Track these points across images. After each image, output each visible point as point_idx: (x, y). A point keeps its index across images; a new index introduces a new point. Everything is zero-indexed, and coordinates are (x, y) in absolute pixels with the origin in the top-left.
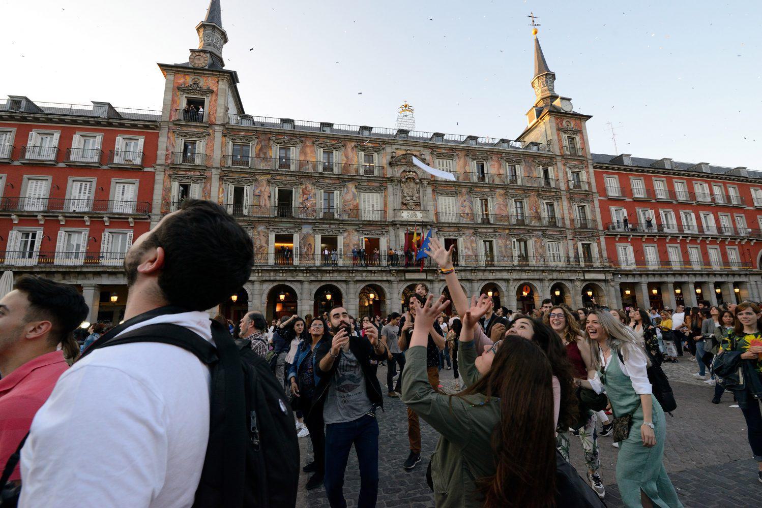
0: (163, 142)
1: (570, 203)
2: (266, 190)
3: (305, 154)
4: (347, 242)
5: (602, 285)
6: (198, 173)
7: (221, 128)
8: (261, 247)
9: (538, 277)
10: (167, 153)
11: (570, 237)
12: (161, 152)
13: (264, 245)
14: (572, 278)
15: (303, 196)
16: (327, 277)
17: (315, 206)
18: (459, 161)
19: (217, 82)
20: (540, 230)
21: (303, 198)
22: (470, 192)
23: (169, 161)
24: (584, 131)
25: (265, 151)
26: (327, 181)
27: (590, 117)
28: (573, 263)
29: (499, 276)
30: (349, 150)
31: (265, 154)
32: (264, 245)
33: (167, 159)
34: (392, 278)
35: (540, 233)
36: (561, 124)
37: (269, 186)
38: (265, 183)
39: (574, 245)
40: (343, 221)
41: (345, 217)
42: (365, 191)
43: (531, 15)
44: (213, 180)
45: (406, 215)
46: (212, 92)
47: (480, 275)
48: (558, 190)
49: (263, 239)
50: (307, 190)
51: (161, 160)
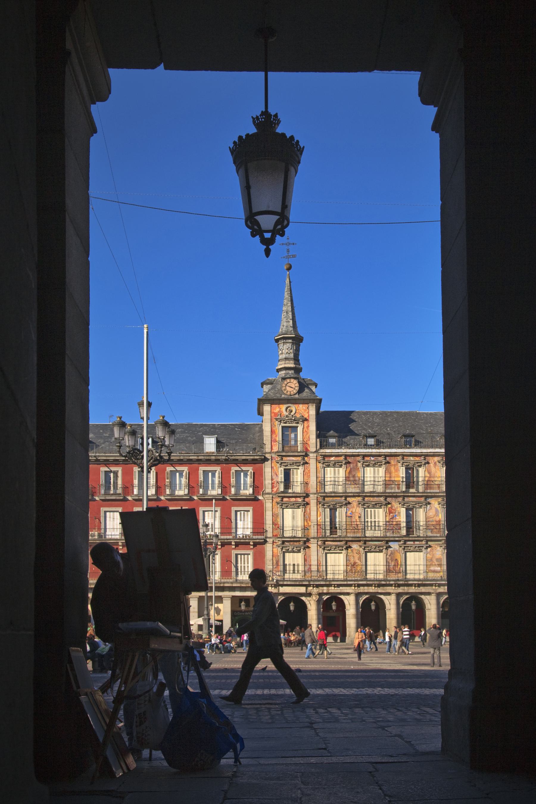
2: (357, 511)
7: (315, 455)
8: (355, 563)
12: (268, 482)
13: (357, 561)
16: (412, 590)
19: (308, 408)
23: (275, 489)
26: (411, 499)
30: (432, 465)
31: (354, 476)
38: (355, 504)
40: (427, 537)
44: (311, 505)
50: (393, 508)
51: (268, 490)
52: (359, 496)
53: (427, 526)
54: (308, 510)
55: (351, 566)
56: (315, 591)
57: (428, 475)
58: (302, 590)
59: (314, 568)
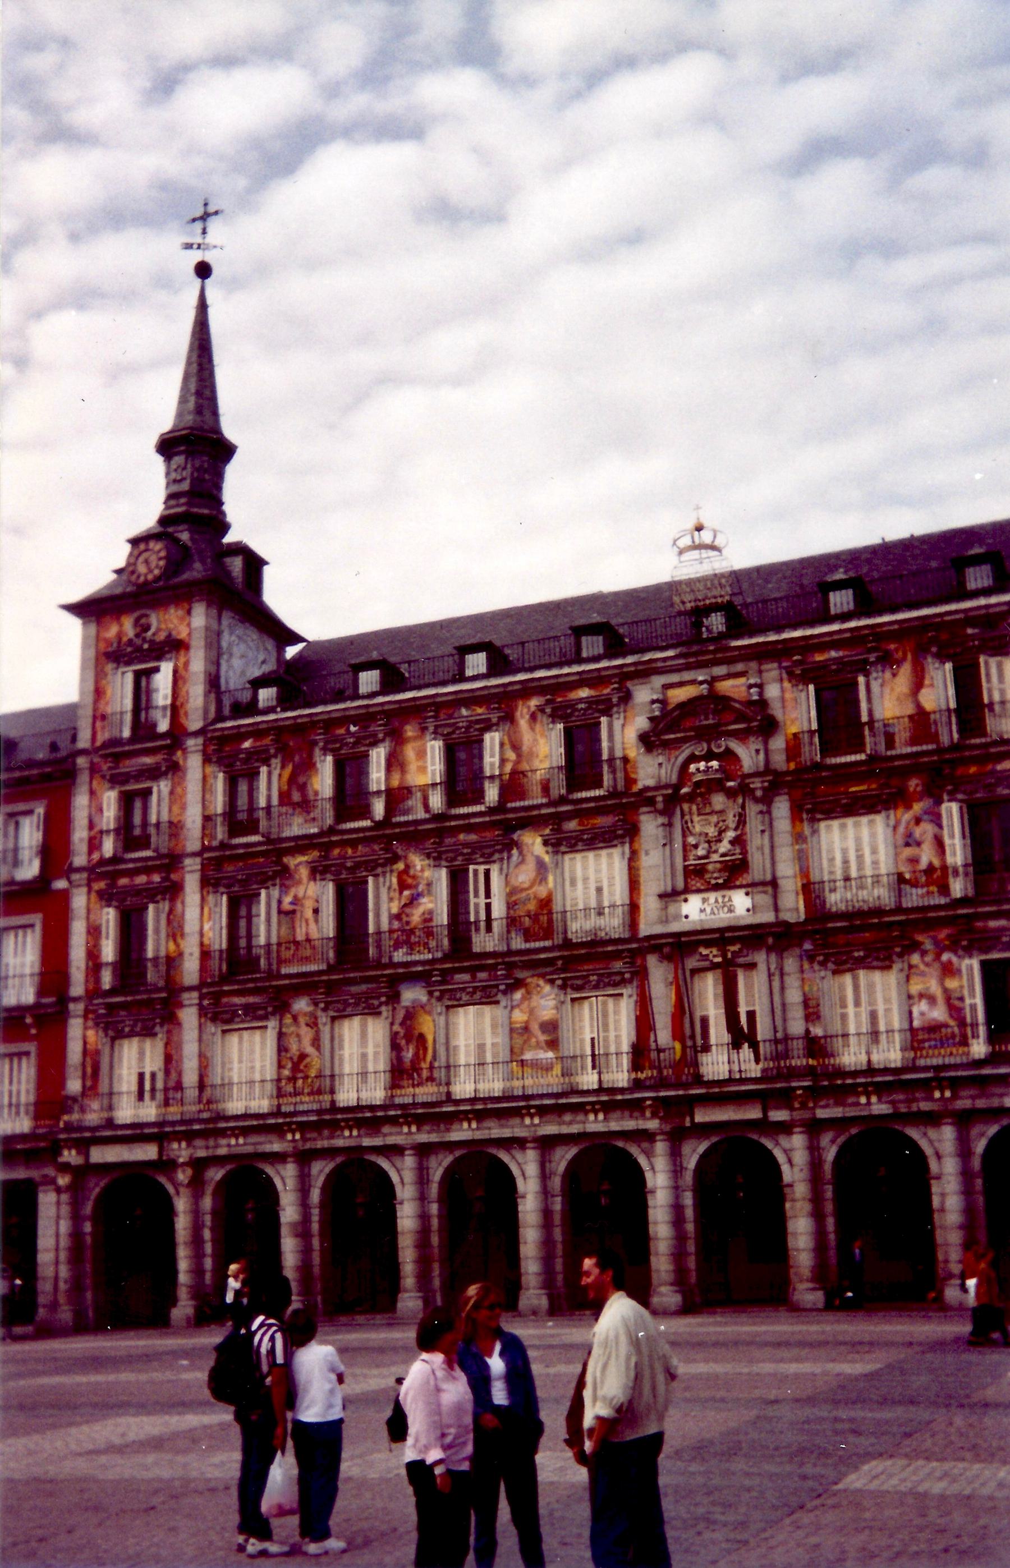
3: (403, 767)
4: (519, 1016)
6: (156, 878)
8: (303, 1056)
10: (93, 833)
12: (80, 835)
13: (310, 1050)
15: (401, 893)
17: (431, 920)
18: (894, 675)
21: (400, 900)
23: (96, 856)
25: (301, 780)
26: (462, 837)
30: (523, 723)
31: (303, 788)
32: (310, 1050)
34: (653, 1125)
37: (315, 880)
38: (304, 872)
40: (510, 953)
41: (518, 943)
42: (573, 849)
45: (696, 911)
46: (175, 646)
49: (307, 1034)
50: (412, 872)
51: (80, 859)
52: (312, 847)
53: (512, 922)
54: (179, 905)
55: (293, 1067)
56: (181, 1151)
57: (511, 755)
58: (148, 1152)
59: (190, 1078)
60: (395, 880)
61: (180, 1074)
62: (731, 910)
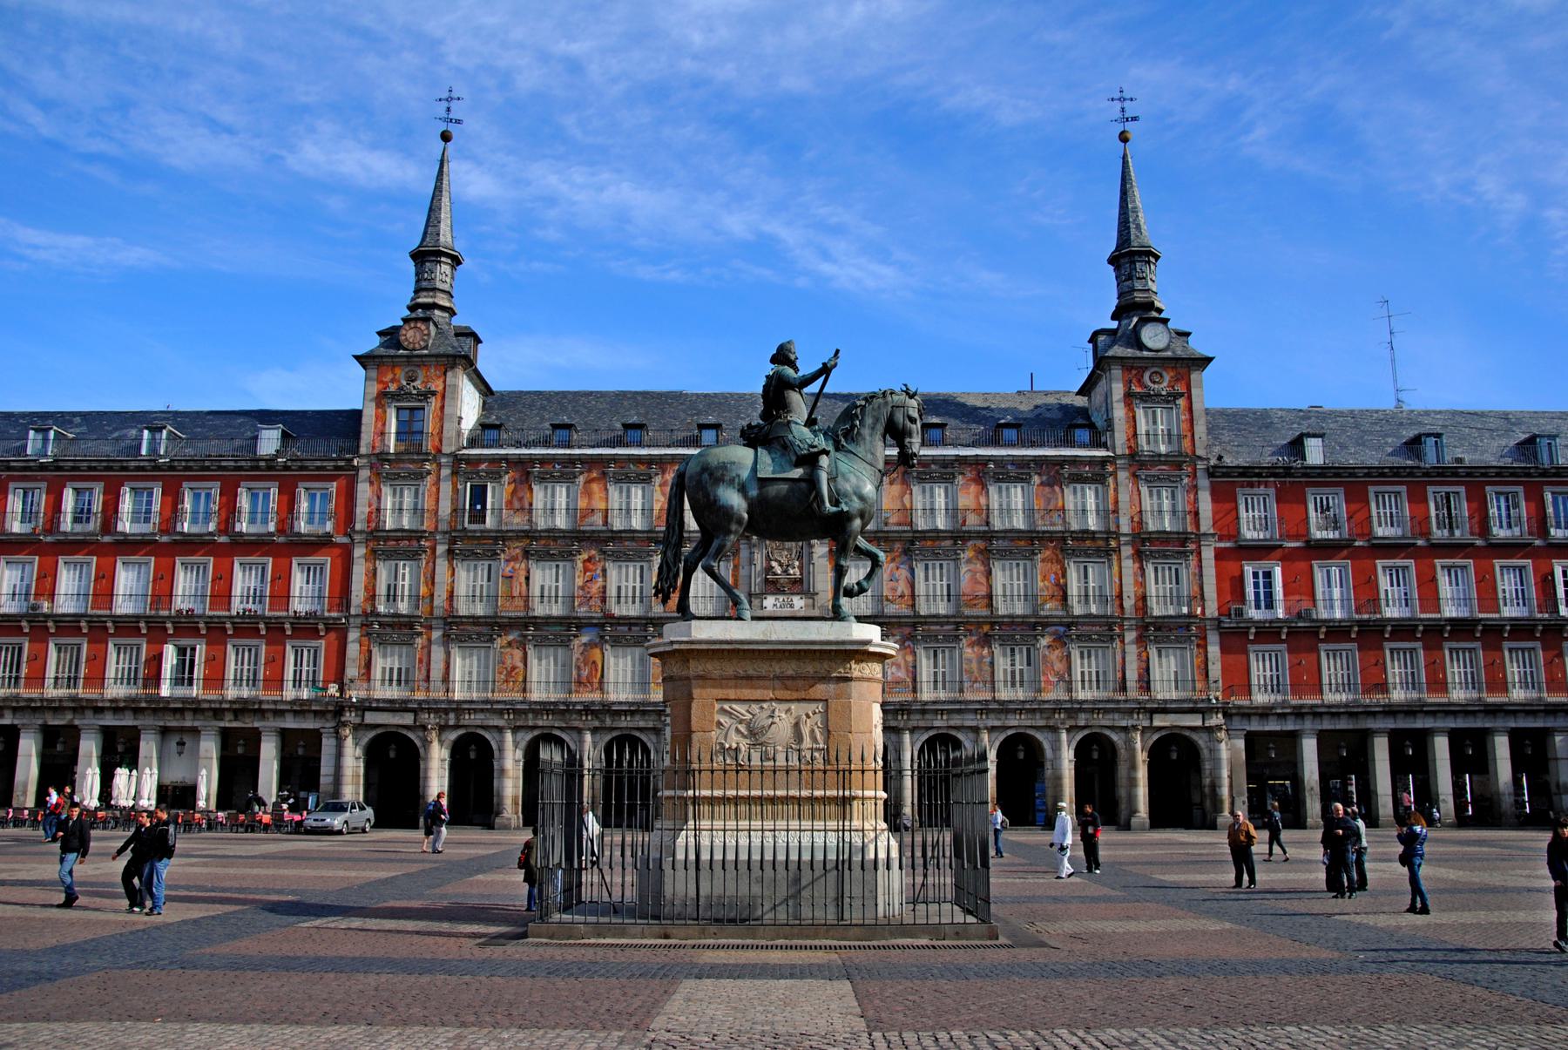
0: (364, 491)
1: (1141, 562)
5: (1201, 740)
8: (514, 668)
9: (1042, 723)
11: (1130, 636)
12: (362, 510)
14: (1124, 723)
20: (1061, 624)
22: (907, 552)
24: (1194, 391)
27: (1210, 360)
28: (1133, 692)
29: (956, 721)
31: (521, 499)
32: (521, 665)
33: (369, 522)
35: (1062, 629)
36: (1140, 382)
39: (1139, 655)
43: (1118, 95)
46: (434, 393)
47: (916, 720)
48: (1111, 534)
49: (518, 654)
56: (431, 720)
58: (408, 719)
59: (436, 674)
60: (580, 565)
61: (428, 671)
62: (792, 606)
